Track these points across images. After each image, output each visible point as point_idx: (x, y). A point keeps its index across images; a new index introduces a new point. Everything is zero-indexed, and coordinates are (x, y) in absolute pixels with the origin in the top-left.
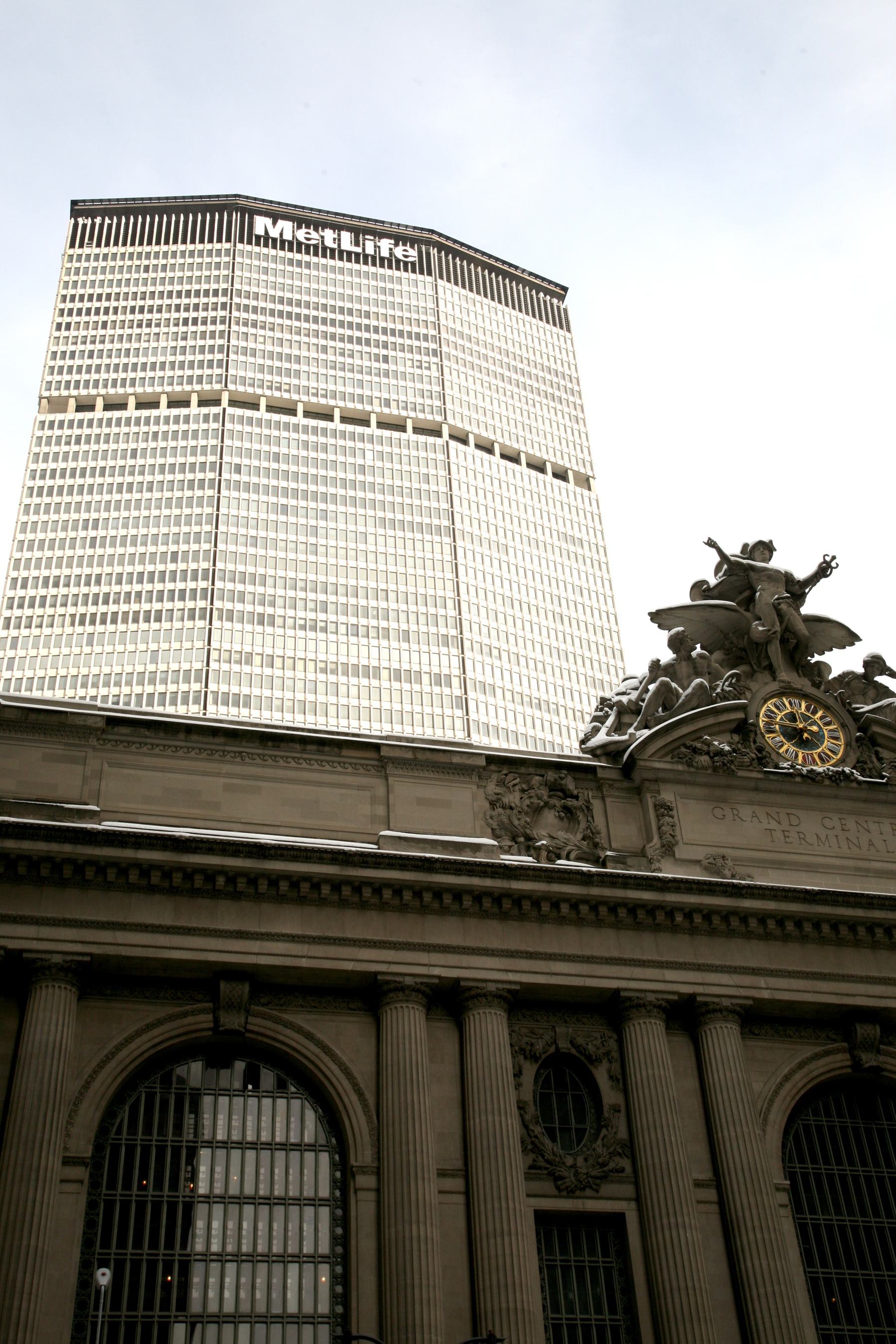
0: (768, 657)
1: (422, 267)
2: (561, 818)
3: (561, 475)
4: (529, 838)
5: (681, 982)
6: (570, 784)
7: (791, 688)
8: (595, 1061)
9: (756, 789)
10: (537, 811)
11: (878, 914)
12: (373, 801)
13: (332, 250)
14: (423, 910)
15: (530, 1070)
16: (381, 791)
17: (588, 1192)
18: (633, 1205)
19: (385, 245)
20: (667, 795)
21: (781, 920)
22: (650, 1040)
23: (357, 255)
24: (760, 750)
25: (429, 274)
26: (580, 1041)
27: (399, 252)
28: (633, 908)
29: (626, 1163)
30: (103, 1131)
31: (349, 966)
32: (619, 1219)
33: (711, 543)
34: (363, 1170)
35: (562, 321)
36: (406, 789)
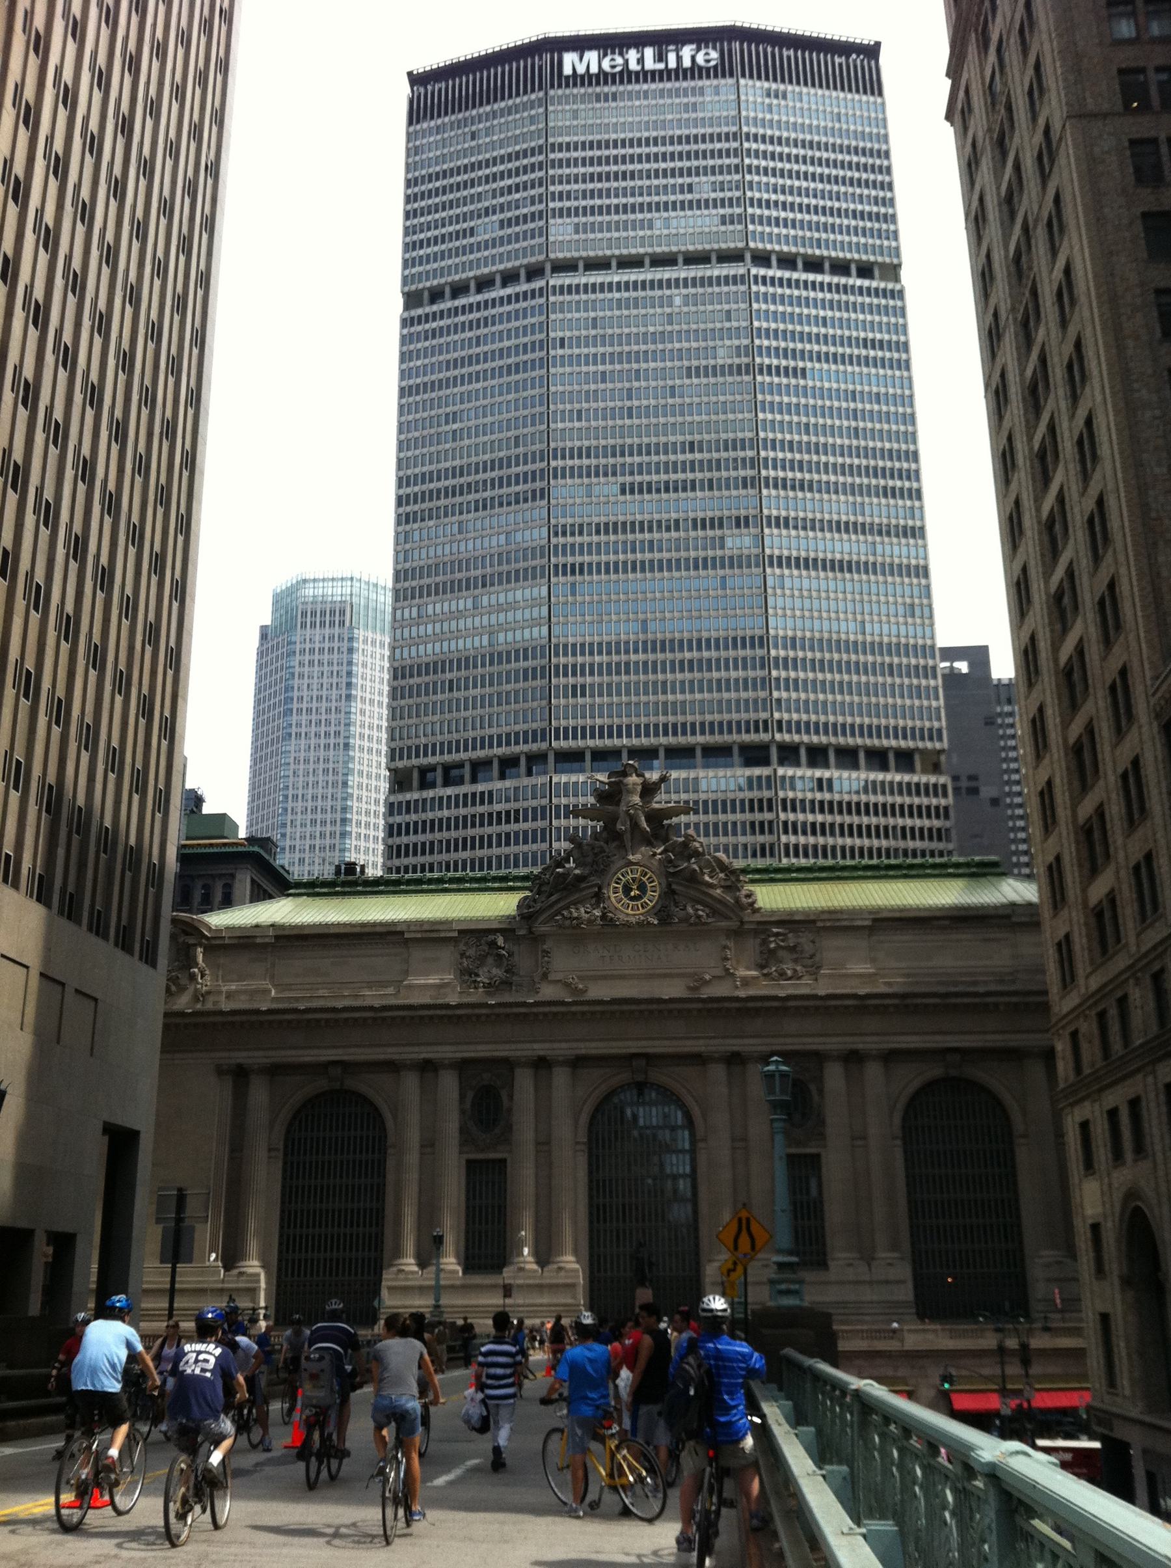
1: (723, 70)
3: (865, 271)
4: (477, 975)
5: (540, 1049)
6: (500, 941)
10: (481, 960)
13: (637, 73)
15: (470, 1095)
19: (687, 51)
23: (661, 72)
25: (731, 75)
27: (700, 59)
28: (517, 1015)
30: (288, 1132)
32: (505, 1160)
35: (874, 86)
36: (417, 954)
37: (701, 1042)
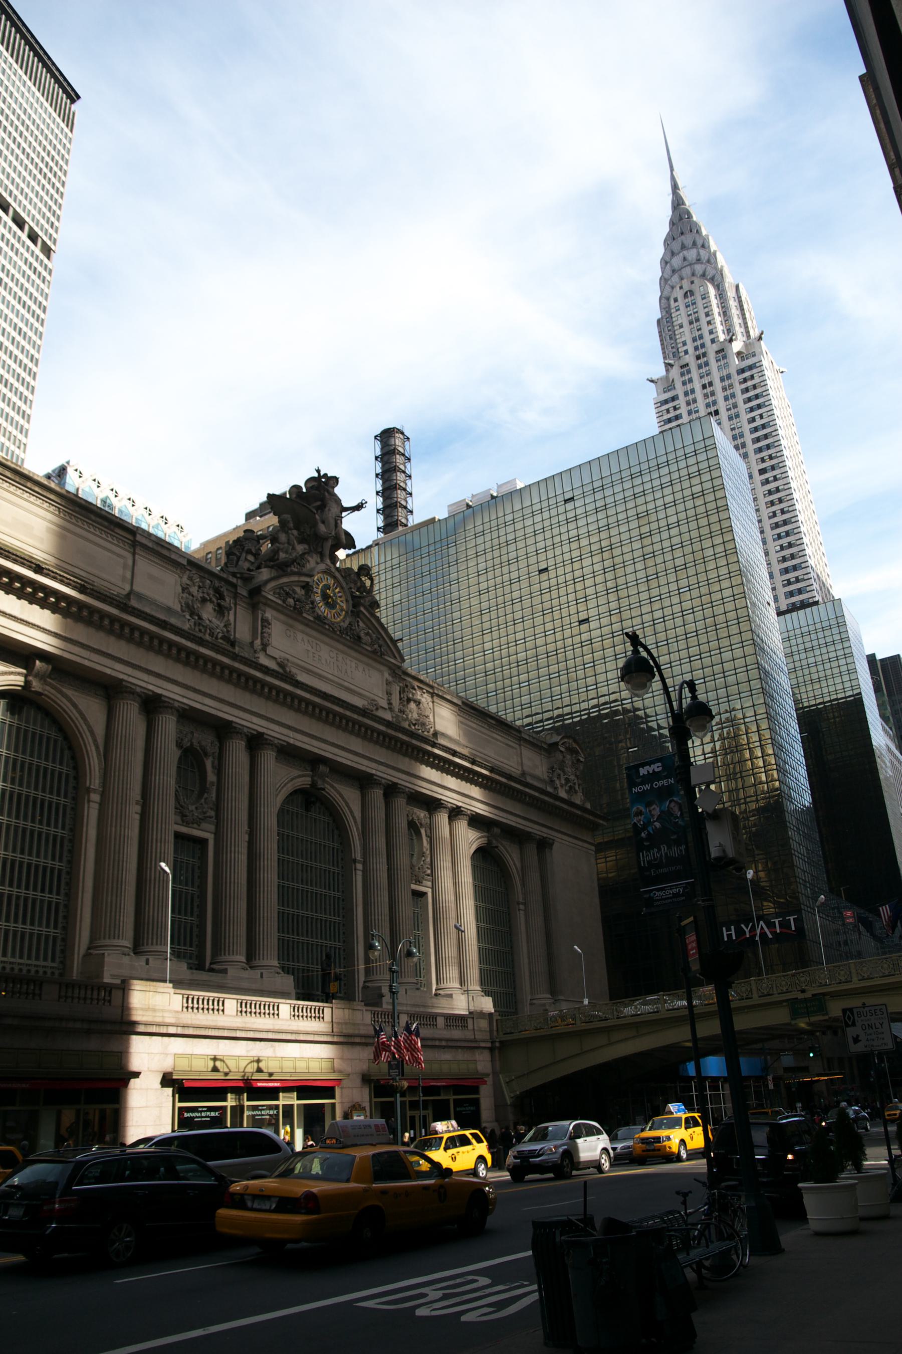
0: (322, 547)
2: (215, 610)
4: (200, 618)
5: (257, 724)
7: (329, 570)
8: (206, 754)
9: (307, 625)
10: (204, 600)
11: (348, 713)
12: (125, 567)
14: (150, 648)
16: (130, 562)
17: (195, 825)
18: (213, 836)
20: (269, 614)
21: (308, 702)
22: (238, 752)
24: (312, 603)
26: (203, 743)
29: (213, 813)
31: (108, 671)
33: (318, 471)
34: (95, 791)
36: (146, 566)
37: (374, 765)
